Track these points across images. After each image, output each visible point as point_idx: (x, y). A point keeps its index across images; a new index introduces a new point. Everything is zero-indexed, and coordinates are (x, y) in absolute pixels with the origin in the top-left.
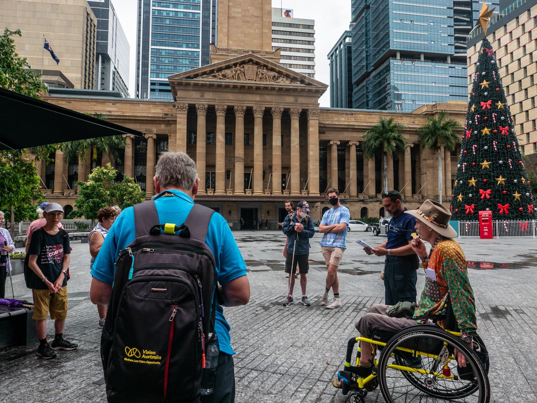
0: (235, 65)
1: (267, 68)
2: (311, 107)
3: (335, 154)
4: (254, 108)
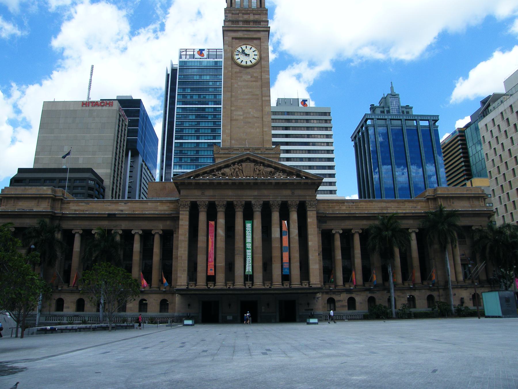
0: (234, 164)
1: (264, 165)
2: (308, 199)
3: (338, 243)
4: (253, 202)
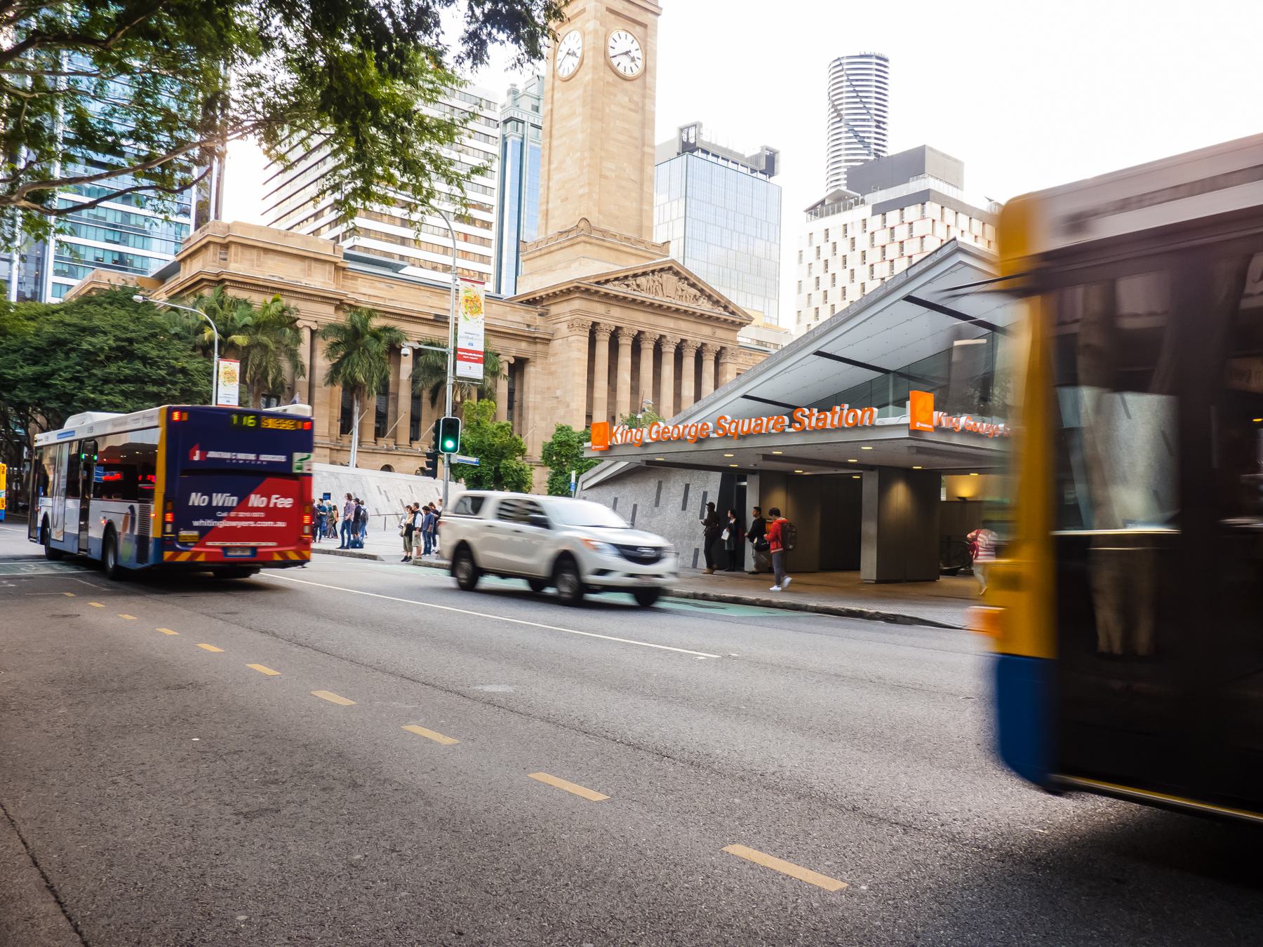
2: (729, 346)
